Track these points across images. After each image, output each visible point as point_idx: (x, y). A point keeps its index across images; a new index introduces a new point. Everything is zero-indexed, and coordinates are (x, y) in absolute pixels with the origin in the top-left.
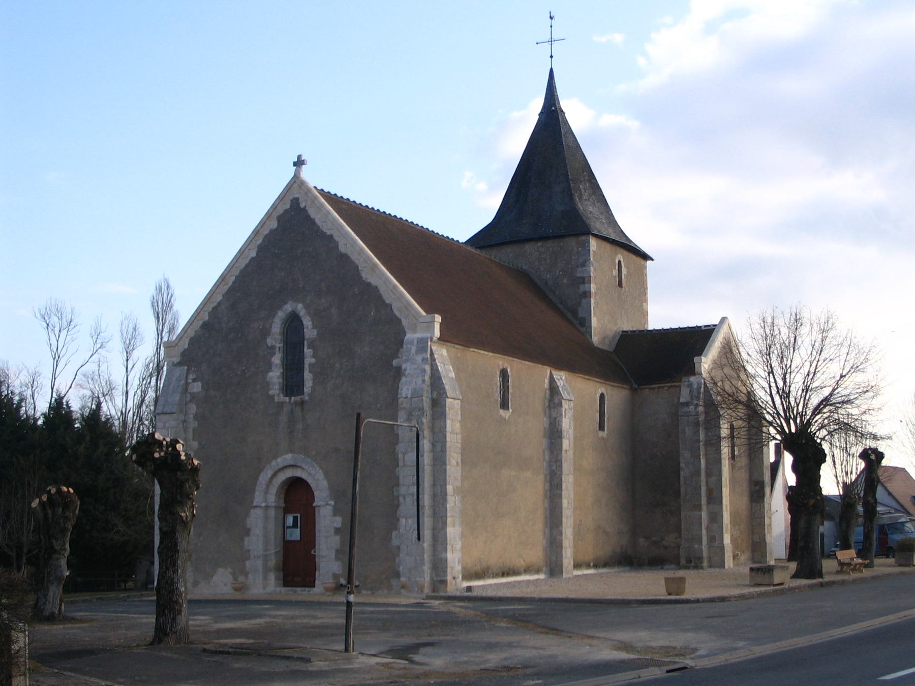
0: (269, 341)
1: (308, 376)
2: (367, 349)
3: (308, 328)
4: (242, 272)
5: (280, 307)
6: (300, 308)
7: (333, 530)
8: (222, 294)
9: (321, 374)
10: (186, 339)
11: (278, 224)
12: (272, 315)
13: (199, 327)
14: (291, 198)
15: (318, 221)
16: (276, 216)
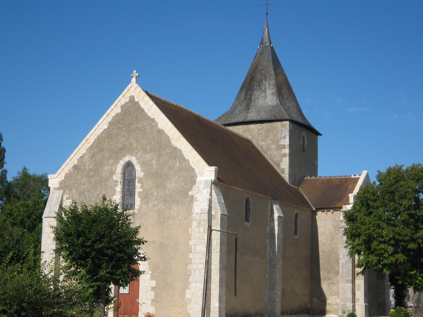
0: (115, 178)
1: (137, 199)
2: (173, 184)
3: (138, 171)
4: (98, 137)
5: (121, 159)
6: (134, 160)
7: (150, 288)
8: (86, 149)
9: (145, 198)
10: (63, 174)
11: (121, 110)
12: (116, 162)
13: (71, 167)
14: (130, 95)
15: (146, 110)
16: (121, 105)
